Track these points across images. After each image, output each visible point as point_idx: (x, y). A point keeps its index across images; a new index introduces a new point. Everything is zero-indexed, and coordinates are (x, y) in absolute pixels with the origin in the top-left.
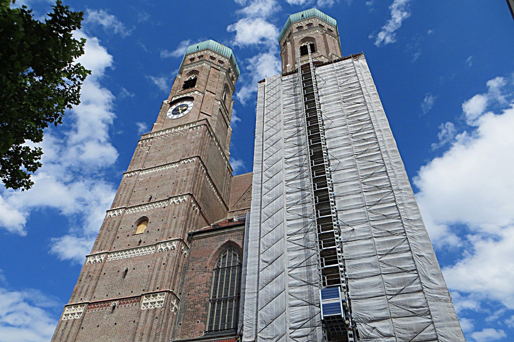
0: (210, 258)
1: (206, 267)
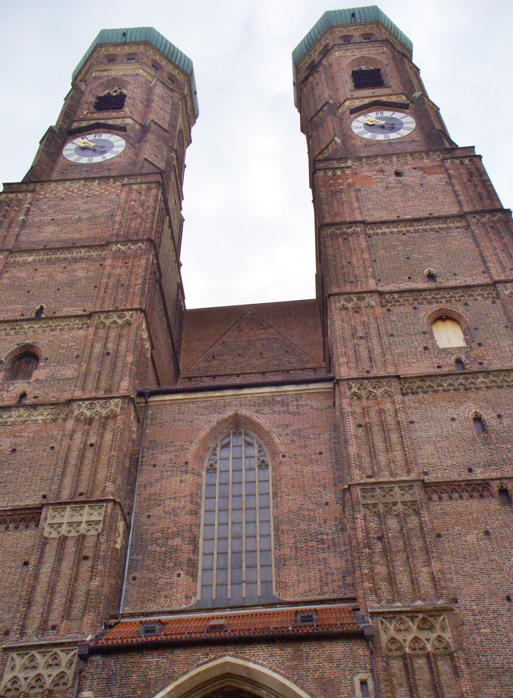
0: (194, 447)
1: (186, 463)
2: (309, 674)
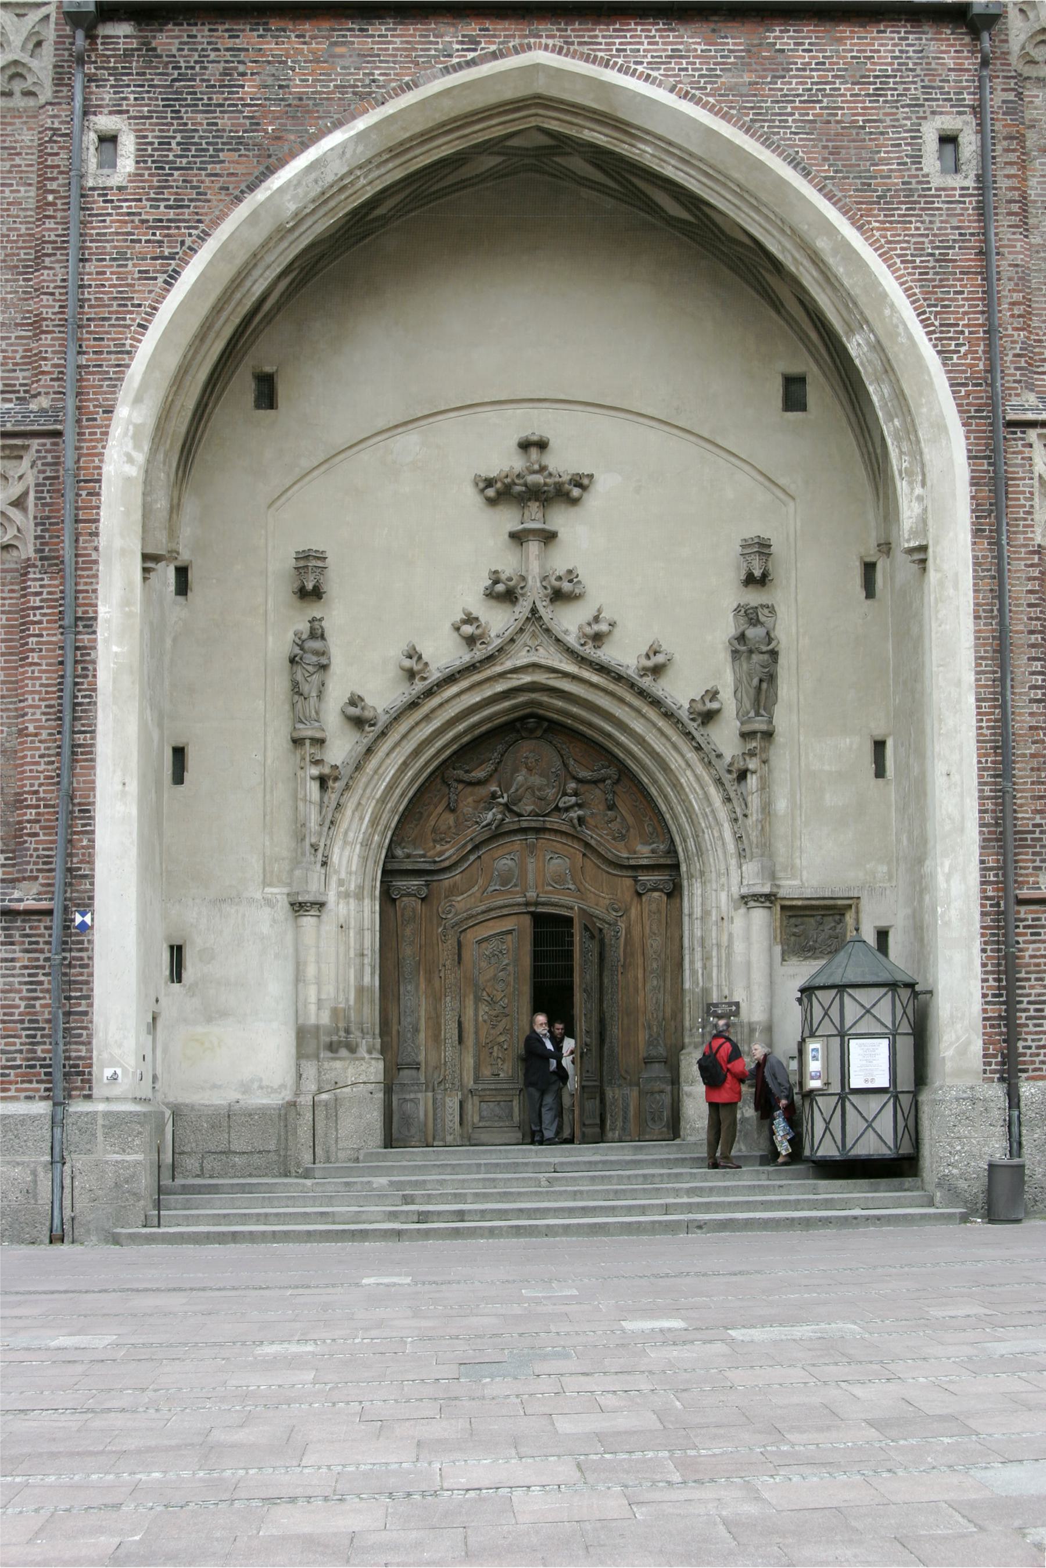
2: (789, 110)
